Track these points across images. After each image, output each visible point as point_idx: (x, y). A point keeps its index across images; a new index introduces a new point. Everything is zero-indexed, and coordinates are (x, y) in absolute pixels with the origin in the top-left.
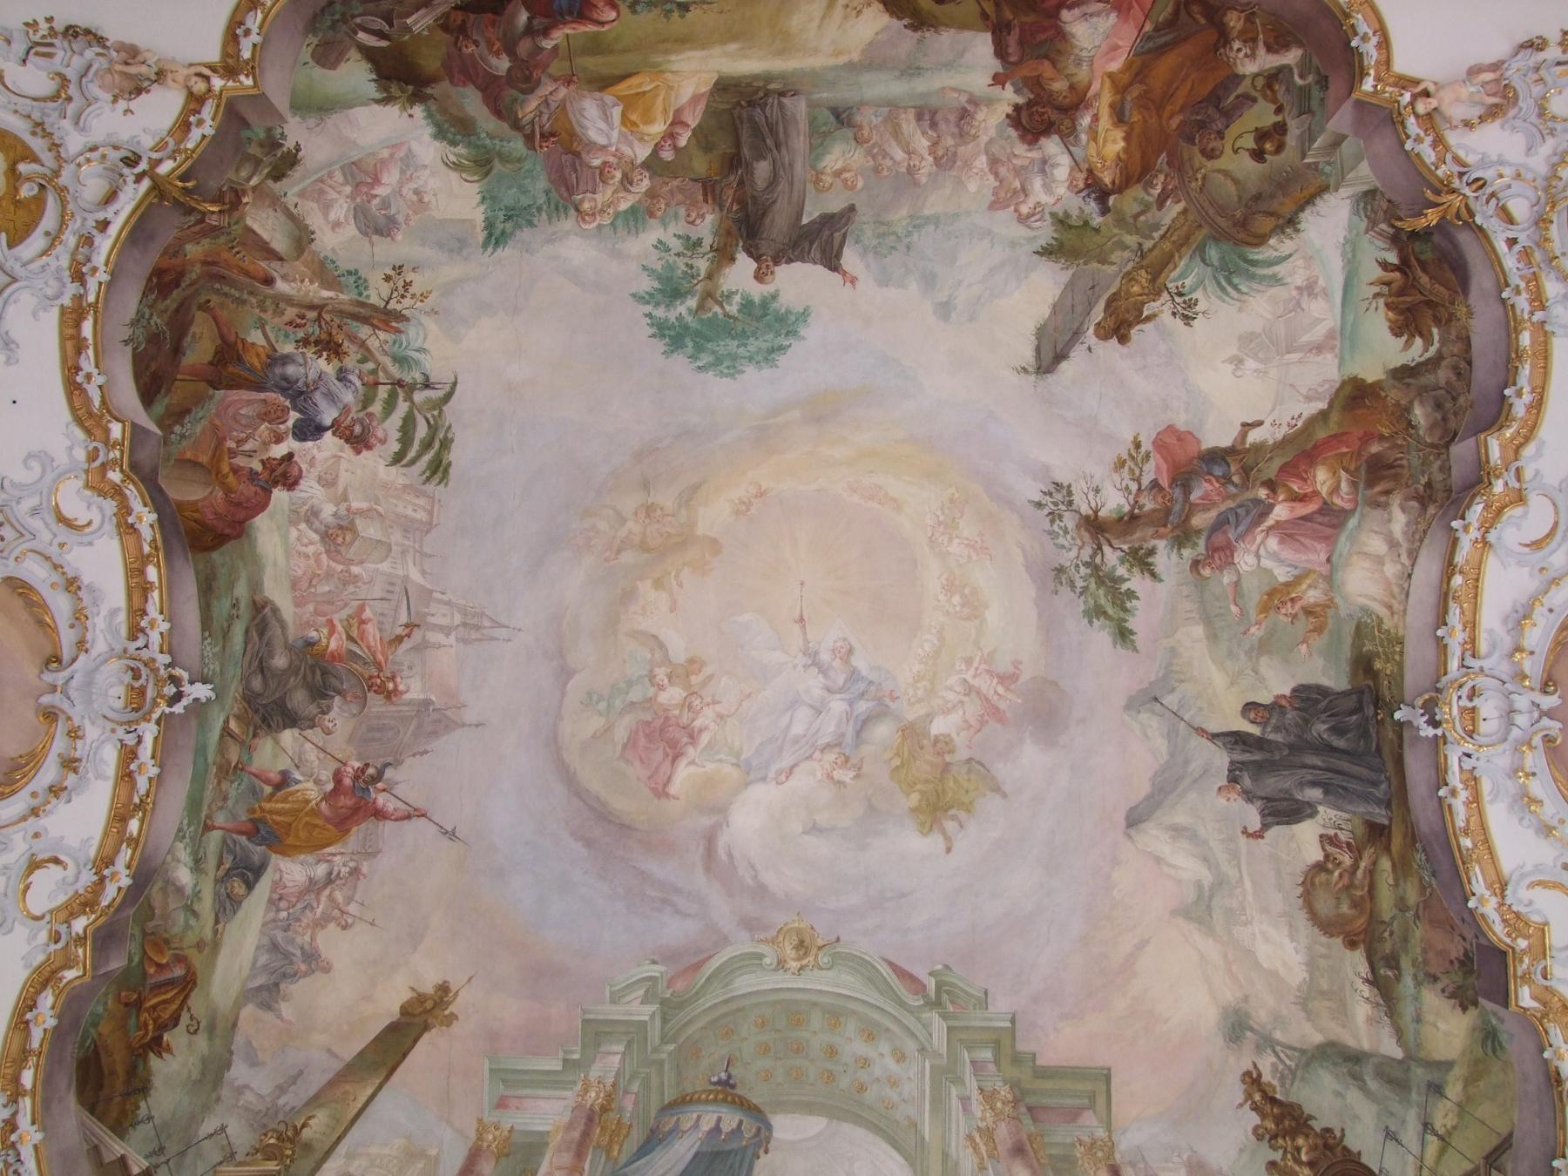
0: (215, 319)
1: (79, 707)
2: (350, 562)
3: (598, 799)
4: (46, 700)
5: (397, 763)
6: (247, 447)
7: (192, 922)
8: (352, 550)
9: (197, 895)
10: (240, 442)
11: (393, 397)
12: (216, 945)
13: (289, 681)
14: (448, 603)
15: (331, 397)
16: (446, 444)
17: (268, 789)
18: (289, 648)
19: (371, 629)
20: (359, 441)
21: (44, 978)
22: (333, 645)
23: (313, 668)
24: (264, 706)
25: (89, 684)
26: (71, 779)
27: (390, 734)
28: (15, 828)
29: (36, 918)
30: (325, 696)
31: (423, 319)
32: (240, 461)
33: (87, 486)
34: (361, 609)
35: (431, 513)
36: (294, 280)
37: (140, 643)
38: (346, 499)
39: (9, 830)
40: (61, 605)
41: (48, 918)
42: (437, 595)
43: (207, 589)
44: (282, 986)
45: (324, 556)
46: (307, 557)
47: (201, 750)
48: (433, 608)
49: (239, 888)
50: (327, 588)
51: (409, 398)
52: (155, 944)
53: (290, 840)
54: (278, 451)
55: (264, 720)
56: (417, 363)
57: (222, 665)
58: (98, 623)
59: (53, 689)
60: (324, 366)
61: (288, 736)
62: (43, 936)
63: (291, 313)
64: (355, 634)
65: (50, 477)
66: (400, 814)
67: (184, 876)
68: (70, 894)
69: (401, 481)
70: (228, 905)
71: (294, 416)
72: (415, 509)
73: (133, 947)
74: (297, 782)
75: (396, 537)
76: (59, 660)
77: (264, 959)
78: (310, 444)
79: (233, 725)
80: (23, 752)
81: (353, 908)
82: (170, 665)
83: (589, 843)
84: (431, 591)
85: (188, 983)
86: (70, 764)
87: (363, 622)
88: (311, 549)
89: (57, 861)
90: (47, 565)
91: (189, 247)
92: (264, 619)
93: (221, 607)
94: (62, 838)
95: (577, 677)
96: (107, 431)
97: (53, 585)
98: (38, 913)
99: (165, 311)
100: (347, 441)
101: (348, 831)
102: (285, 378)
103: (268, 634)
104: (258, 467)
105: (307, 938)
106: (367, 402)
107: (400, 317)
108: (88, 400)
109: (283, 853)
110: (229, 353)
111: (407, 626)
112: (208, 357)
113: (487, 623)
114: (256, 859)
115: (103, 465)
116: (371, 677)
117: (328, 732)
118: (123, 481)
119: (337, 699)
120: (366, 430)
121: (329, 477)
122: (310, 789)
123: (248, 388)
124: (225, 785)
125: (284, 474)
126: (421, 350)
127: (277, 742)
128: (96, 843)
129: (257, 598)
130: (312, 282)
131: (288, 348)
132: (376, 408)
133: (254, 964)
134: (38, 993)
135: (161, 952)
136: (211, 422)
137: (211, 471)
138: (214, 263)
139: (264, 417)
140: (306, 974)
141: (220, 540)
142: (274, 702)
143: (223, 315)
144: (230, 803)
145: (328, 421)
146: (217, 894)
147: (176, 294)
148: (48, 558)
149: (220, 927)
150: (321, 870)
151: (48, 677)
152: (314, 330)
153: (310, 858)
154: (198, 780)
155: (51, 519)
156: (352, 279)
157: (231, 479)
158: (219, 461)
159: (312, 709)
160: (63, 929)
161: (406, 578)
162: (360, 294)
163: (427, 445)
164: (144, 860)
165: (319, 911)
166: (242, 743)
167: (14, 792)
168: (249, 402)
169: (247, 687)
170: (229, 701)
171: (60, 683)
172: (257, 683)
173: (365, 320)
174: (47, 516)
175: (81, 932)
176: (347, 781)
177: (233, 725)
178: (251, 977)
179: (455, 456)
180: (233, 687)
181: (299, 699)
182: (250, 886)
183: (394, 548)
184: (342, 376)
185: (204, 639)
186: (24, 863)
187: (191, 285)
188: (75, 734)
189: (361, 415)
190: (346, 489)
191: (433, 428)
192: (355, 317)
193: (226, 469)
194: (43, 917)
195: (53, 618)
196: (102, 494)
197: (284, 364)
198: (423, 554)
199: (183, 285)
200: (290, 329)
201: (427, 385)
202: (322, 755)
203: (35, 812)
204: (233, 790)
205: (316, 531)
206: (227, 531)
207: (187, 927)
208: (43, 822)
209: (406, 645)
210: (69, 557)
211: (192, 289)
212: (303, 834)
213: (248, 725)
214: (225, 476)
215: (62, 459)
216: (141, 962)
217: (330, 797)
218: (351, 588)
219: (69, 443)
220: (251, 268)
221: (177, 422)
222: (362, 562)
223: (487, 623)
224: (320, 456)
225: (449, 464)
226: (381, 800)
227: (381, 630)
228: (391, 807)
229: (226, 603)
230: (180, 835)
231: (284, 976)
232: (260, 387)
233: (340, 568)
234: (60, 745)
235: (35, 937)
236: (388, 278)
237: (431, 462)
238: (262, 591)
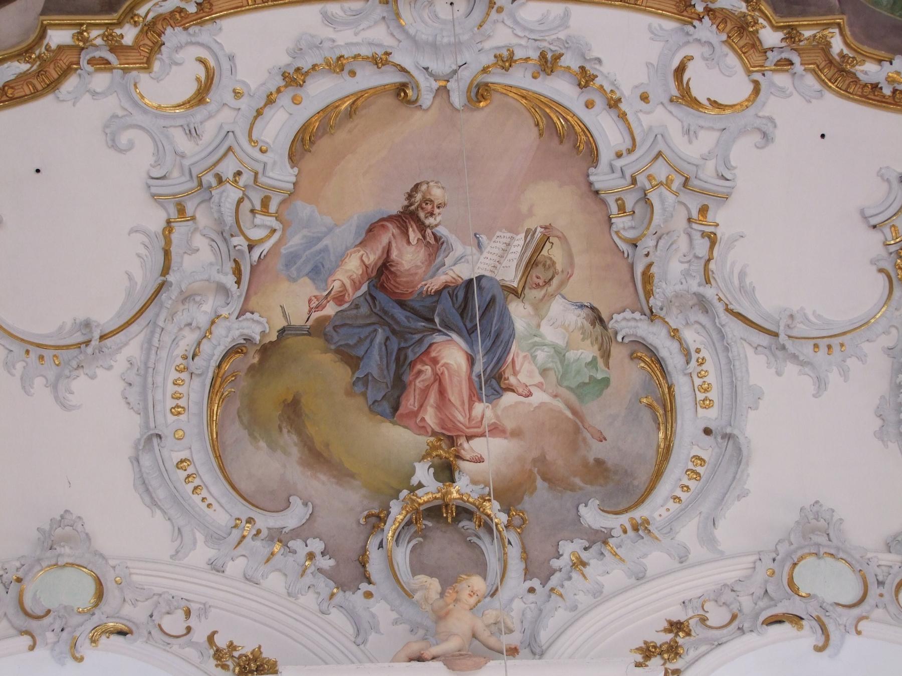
1: (467, 56)
4: (457, 99)
21: (840, 76)
25: (435, 48)
26: (570, 61)
28: (634, 125)
29: (757, 90)
33: (147, 66)
39: (637, 132)
40: (322, 91)
41: (757, 76)
58: (346, 40)
59: (443, 91)
62: (781, 79)
65: (139, 118)
68: (726, 49)
76: (401, 89)
80: (531, 123)
86: (548, 64)
89: (680, 71)
90: (268, 112)
94: (648, 65)
96: (61, 48)
97: (296, 101)
98: (751, 87)
108: (22, 77)
115: (112, 50)
118: (136, 24)
128: (656, 21)
134: (856, 81)
148: (259, 113)
151: (426, 99)
155: (200, 113)
160: (773, 57)
167: (586, 130)
171: (435, 85)
174: (199, 117)
175: (780, 35)
186: (684, 113)
188: (506, 61)
194: (756, 84)
195: (342, 100)
196: (157, 46)
203: (614, 104)
208: (627, 91)
210: (253, 87)
215: (112, 104)
219: (87, 96)
234: (520, 78)
235: (782, 90)
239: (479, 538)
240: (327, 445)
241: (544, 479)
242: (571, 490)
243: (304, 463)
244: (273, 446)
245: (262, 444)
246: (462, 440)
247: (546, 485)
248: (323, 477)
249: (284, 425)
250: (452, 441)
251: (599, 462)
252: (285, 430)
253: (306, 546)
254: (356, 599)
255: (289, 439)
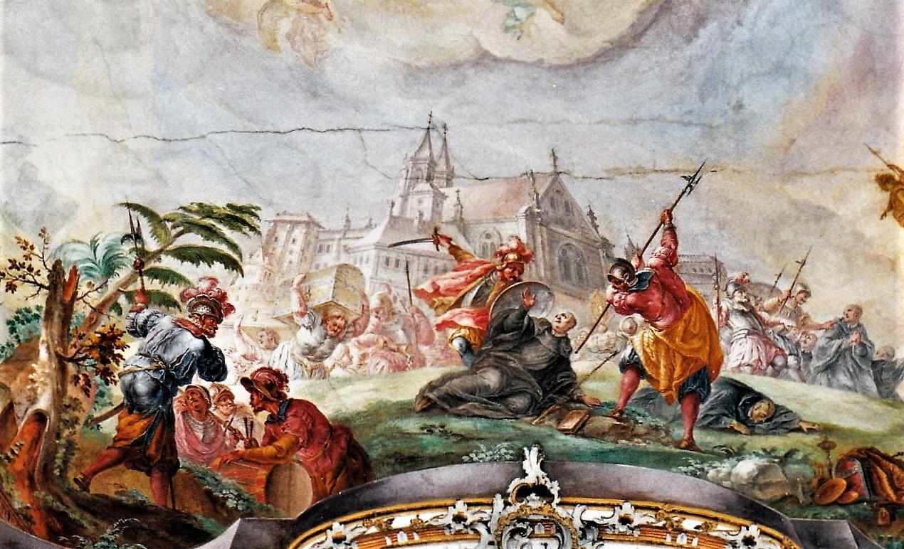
0: (95, 473)
2: (365, 309)
3: (642, 13)
5: (606, 245)
6: (242, 429)
7: (799, 456)
8: (350, 307)
9: (768, 453)
10: (236, 435)
11: (155, 274)
12: (827, 430)
13: (517, 366)
14: (405, 197)
15: (168, 342)
16: (206, 211)
17: (643, 384)
18: (474, 369)
19: (445, 281)
20: (218, 308)
22: (468, 322)
23: (497, 343)
24: (545, 393)
27: (570, 254)
30: (530, 329)
31: (55, 243)
32: (259, 434)
34: (421, 294)
35: (296, 224)
36: (34, 390)
37: (481, 529)
38: (291, 318)
42: (396, 212)
43: (411, 461)
44: (876, 358)
45: (362, 338)
46: (364, 356)
47: (601, 457)
48: (411, 214)
49: (760, 409)
50: (400, 333)
51: (156, 255)
52: (824, 494)
53: (704, 357)
54: (242, 396)
55: (562, 392)
56: (110, 248)
57: (500, 440)
60: (131, 351)
61: (579, 365)
63: (73, 391)
64: (452, 299)
66: (669, 240)
67: (746, 468)
69: (259, 258)
70: (780, 420)
71: (197, 380)
72: (292, 246)
73: (826, 517)
74: (633, 352)
75: (329, 259)
77: (843, 379)
78: (228, 362)
79: (569, 425)
81: (784, 286)
82: (505, 495)
83: (701, 20)
84: (392, 217)
85: (870, 457)
87: (437, 291)
88: (355, 353)
91: (17, 506)
92: (442, 398)
93: (434, 445)
95: (486, 46)
99: (96, 525)
100: (220, 321)
101: (690, 295)
102: (153, 393)
103: (460, 393)
104: (263, 416)
105: (820, 333)
106: (167, 302)
107: (56, 271)
109: (719, 363)
110: (130, 454)
111: (437, 243)
112: (142, 476)
113: (426, 153)
114: (724, 392)
116: (503, 279)
117: (572, 323)
119: (532, 314)
120: (202, 300)
121: (265, 338)
122: (643, 339)
123: (172, 431)
124: (641, 430)
125: (268, 387)
126: (94, 245)
127: (586, 377)
129: (418, 408)
130: (33, 371)
131: (117, 392)
132: (174, 291)
133: (850, 389)
135: (834, 486)
136: (219, 468)
137: (276, 468)
138: (31, 478)
139: (204, 413)
140: (863, 334)
141: (354, 450)
142: (540, 383)
143: (89, 464)
144: (661, 423)
145: (198, 343)
146: (767, 432)
147: (75, 515)
149: (805, 427)
150: (739, 323)
152: (89, 365)
153: (725, 334)
154: (636, 458)
156: (20, 327)
157: (282, 443)
158: (261, 457)
159: (546, 340)
161: (378, 246)
162: (37, 317)
163: (210, 232)
164: (729, 509)
165: (787, 322)
166: (591, 414)
168: (189, 429)
169: (525, 412)
170: (544, 430)
172: (519, 402)
173: (68, 310)
176: (631, 298)
177: (569, 425)
178: (865, 391)
179: (220, 199)
180: (526, 427)
181: (535, 356)
182: (759, 397)
183: (344, 259)
184: (140, 331)
185: (471, 461)
187: (60, 499)
189: (184, 307)
190: (277, 319)
191: (190, 226)
192: (66, 321)
193: (270, 449)
197: (136, 394)
198: (348, 228)
199: (62, 508)
200: (93, 391)
201: (137, 236)
202: (600, 328)
204: (645, 421)
205: (332, 348)
206: (343, 444)
207: (805, 460)
209: (460, 241)
211: (66, 499)
212: (696, 344)
213: (569, 409)
214: (279, 449)
216: (843, 506)
217: (651, 319)
218: (398, 306)
220: (28, 438)
221: (224, 505)
222: (364, 296)
223: (426, 153)
224: (242, 350)
225: (230, 206)
226: (651, 260)
227: (445, 271)
228: (661, 250)
229: (428, 438)
230: (699, 474)
231: (864, 356)
232: (170, 419)
233: (373, 320)
236: (11, 287)
237: (232, 228)
238: (410, 403)
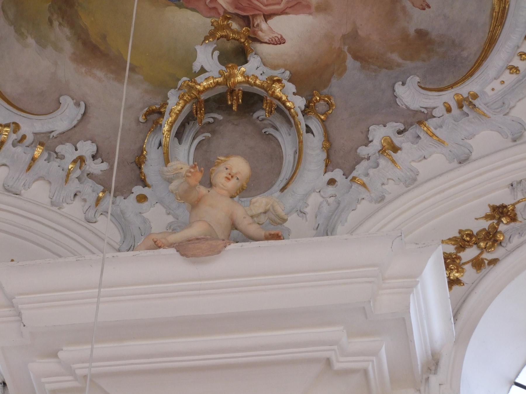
239: (277, 129)
240: (104, 37)
241: (356, 57)
242: (386, 68)
243: (78, 59)
244: (42, 42)
245: (31, 41)
246: (259, 20)
247: (358, 64)
248: (99, 74)
249: (55, 16)
250: (247, 21)
251: (421, 34)
252: (56, 23)
253: (76, 150)
254: (128, 204)
255: (61, 33)
